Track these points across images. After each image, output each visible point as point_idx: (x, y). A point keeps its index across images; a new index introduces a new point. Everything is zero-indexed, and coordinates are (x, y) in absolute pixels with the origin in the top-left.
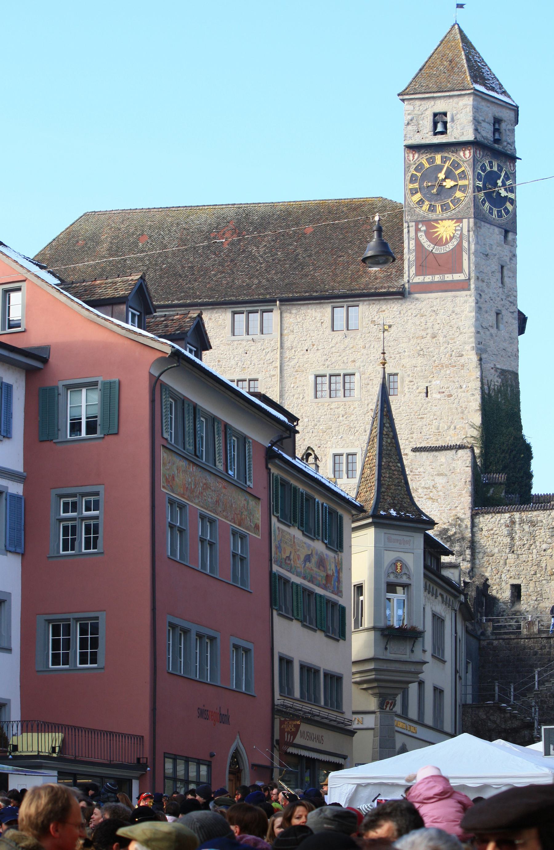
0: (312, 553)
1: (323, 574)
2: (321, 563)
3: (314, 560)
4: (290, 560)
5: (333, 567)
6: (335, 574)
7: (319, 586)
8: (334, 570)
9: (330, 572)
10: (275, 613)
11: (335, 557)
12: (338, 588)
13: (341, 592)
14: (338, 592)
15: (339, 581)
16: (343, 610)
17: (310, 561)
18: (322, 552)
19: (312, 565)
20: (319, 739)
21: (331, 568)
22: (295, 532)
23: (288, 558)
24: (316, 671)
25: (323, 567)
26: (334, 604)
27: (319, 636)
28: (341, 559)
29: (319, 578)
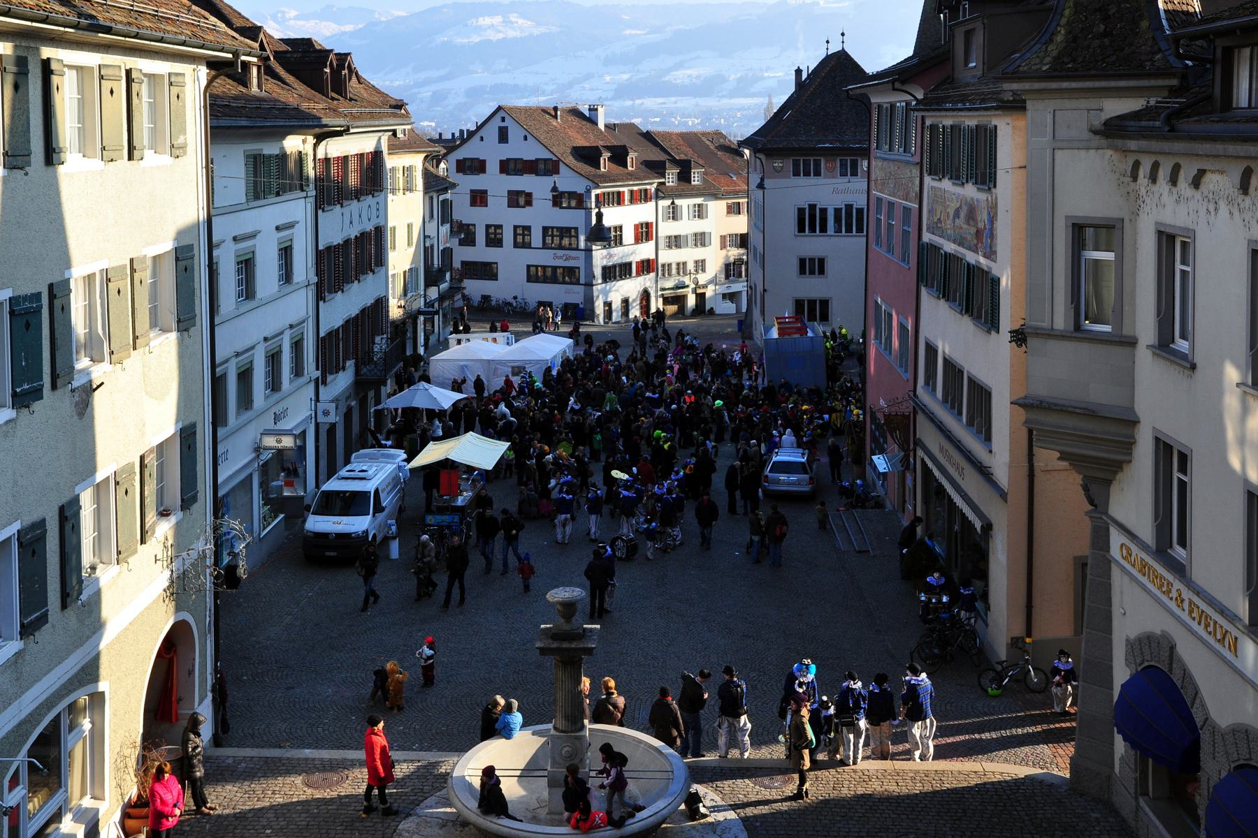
0: (961, 205)
1: (973, 230)
2: (971, 216)
3: (963, 214)
4: (941, 222)
5: (985, 217)
6: (987, 227)
7: (970, 249)
8: (986, 221)
9: (981, 225)
10: (924, 291)
11: (987, 200)
12: (991, 247)
13: (995, 253)
14: (991, 254)
15: (992, 236)
16: (996, 282)
17: (958, 217)
18: (972, 199)
19: (960, 222)
20: (961, 472)
21: (983, 216)
22: (946, 184)
23: (939, 219)
24: (961, 372)
25: (973, 219)
26: (985, 273)
27: (966, 323)
28: (996, 198)
29: (969, 237)
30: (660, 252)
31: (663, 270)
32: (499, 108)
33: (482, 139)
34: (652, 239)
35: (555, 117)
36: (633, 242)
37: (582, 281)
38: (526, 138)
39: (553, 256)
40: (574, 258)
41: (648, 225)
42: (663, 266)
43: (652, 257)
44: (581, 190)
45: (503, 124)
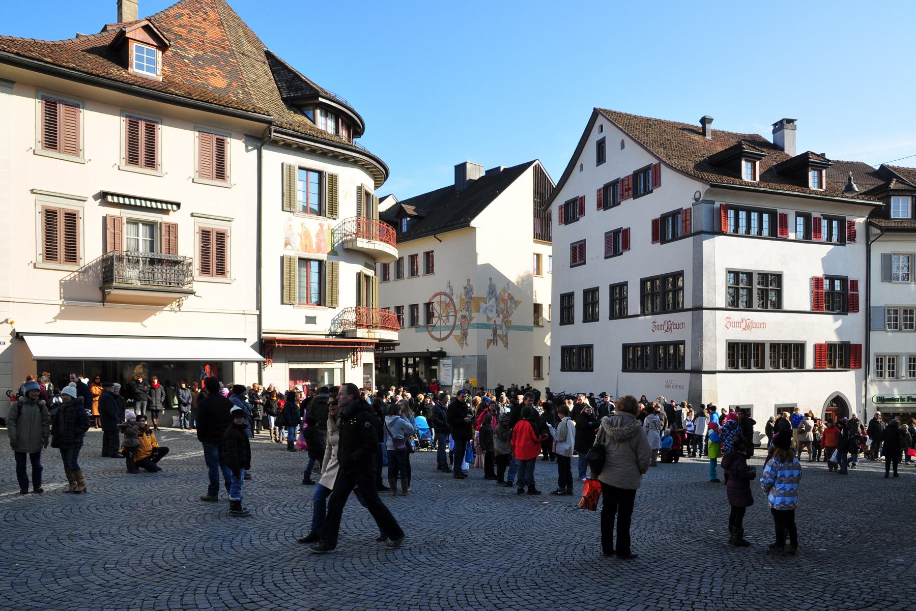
30: (874, 335)
31: (880, 368)
32: (596, 113)
33: (582, 166)
34: (855, 309)
35: (704, 134)
36: (808, 309)
37: (688, 366)
38: (623, 146)
39: (651, 326)
40: (680, 326)
41: (849, 285)
42: (879, 360)
43: (856, 338)
44: (686, 203)
45: (601, 136)
